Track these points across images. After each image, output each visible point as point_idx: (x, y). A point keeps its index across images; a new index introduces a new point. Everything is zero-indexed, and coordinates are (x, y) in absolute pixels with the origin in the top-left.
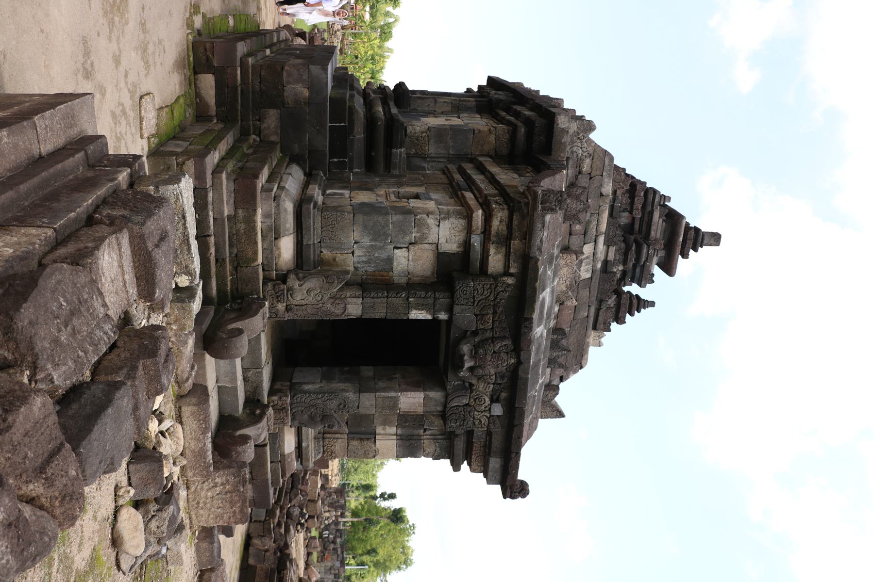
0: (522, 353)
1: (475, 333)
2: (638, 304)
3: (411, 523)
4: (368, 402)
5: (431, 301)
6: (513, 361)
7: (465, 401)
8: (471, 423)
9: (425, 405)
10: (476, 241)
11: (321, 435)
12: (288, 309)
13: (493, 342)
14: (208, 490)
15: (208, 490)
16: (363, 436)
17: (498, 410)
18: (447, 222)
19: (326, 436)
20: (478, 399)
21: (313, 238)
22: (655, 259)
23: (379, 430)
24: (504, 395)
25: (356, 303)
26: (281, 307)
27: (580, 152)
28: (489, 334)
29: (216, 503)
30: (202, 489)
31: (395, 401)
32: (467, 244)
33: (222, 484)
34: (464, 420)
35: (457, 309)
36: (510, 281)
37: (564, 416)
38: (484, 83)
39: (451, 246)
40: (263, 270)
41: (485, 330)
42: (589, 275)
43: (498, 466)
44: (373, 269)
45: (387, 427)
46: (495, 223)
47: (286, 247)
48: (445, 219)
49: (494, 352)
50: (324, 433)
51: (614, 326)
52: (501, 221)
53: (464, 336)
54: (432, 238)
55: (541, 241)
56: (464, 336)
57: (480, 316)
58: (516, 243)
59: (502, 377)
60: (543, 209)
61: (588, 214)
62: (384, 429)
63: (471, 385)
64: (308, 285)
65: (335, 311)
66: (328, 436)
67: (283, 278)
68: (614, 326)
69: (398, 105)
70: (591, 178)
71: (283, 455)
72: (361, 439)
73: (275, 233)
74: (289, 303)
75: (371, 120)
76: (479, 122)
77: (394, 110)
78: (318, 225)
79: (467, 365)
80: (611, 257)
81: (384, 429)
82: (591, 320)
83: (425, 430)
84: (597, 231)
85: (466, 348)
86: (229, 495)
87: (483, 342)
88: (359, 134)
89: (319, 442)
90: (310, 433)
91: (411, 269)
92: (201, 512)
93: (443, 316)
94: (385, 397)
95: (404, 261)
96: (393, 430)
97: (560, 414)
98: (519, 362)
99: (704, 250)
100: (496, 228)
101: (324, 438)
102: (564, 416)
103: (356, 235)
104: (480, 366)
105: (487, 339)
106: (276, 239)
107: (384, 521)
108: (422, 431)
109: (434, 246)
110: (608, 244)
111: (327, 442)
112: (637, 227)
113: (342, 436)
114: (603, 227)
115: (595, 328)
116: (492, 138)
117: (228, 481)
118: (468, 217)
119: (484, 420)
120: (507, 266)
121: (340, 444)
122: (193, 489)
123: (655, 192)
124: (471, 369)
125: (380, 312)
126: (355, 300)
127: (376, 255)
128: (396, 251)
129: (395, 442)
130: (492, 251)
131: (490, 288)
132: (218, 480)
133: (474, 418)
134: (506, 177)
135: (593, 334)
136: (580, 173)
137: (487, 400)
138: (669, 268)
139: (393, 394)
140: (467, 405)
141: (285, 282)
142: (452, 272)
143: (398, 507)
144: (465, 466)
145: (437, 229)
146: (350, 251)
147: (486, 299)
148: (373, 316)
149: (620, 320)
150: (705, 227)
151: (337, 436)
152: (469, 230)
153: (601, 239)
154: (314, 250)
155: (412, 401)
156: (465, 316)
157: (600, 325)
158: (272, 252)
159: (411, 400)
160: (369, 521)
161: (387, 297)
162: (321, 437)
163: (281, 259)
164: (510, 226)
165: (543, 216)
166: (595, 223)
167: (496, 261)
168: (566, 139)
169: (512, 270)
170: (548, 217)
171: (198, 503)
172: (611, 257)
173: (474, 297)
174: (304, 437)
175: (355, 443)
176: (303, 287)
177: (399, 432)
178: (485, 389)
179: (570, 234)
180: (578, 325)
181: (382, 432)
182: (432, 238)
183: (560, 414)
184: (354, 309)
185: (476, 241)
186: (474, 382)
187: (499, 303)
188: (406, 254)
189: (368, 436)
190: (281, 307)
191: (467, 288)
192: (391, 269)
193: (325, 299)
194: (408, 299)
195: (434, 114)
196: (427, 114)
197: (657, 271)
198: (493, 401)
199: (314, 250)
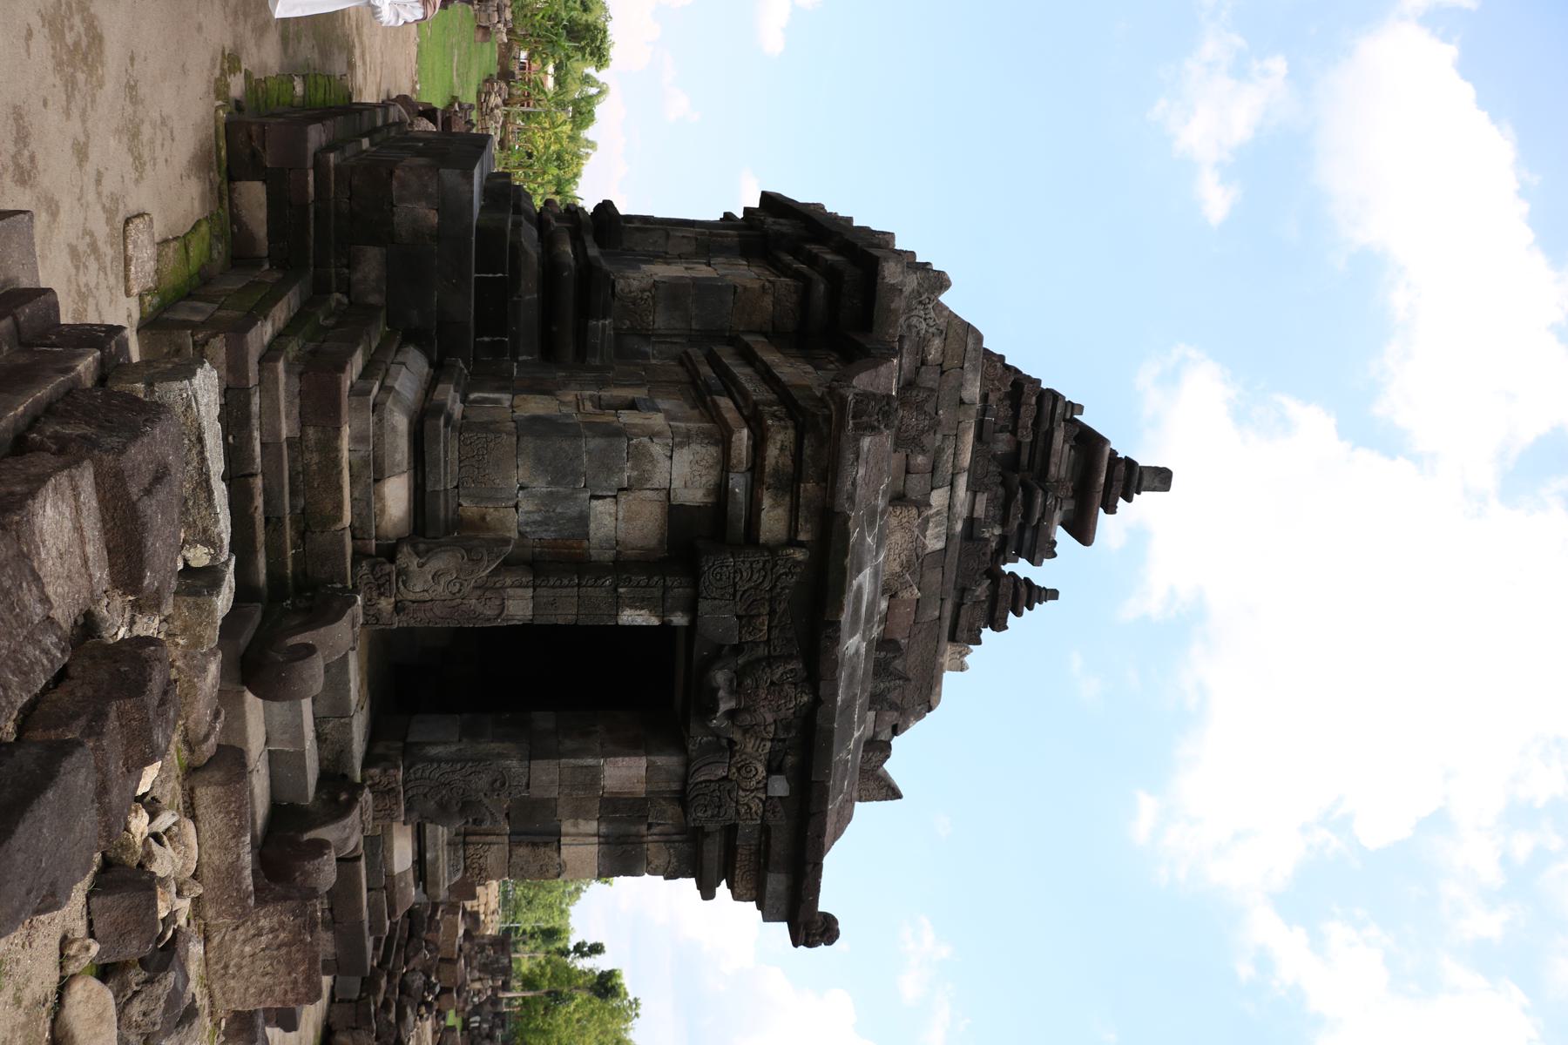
0: (822, 684)
1: (738, 649)
2: (1030, 595)
3: (631, 998)
4: (546, 776)
5: (657, 593)
6: (805, 699)
7: (721, 773)
8: (732, 812)
9: (648, 780)
10: (738, 484)
11: (460, 838)
12: (399, 608)
13: (770, 665)
14: (244, 942)
15: (244, 942)
16: (537, 839)
17: (780, 787)
18: (685, 450)
19: (469, 839)
20: (744, 767)
21: (444, 479)
22: (1058, 516)
23: (567, 827)
24: (790, 760)
25: (522, 598)
26: (386, 604)
27: (924, 326)
28: (762, 651)
29: (262, 965)
30: (234, 939)
31: (595, 773)
32: (721, 491)
33: (272, 930)
34: (720, 807)
35: (704, 606)
36: (800, 555)
37: (899, 796)
38: (755, 203)
39: (694, 494)
40: (353, 538)
41: (756, 644)
42: (940, 545)
43: (782, 888)
44: (553, 535)
45: (581, 822)
46: (772, 452)
47: (396, 496)
48: (681, 445)
49: (772, 683)
50: (466, 834)
51: (987, 633)
52: (782, 449)
53: (717, 654)
54: (660, 479)
55: (854, 484)
56: (717, 654)
57: (746, 619)
58: (808, 488)
59: (787, 728)
60: (857, 427)
61: (939, 437)
62: (576, 825)
63: (731, 742)
64: (437, 563)
65: (484, 611)
66: (473, 839)
67: (389, 552)
68: (987, 633)
69: (601, 244)
70: (942, 373)
71: (390, 876)
72: (534, 845)
73: (374, 471)
74: (400, 597)
75: (550, 267)
76: (744, 274)
77: (593, 251)
78: (454, 455)
79: (724, 707)
80: (980, 512)
81: (576, 825)
82: (947, 624)
83: (650, 826)
84: (954, 466)
85: (720, 677)
86: (284, 951)
88: (529, 292)
89: (456, 851)
91: (621, 536)
92: (232, 983)
93: (679, 619)
94: (575, 767)
95: (609, 521)
97: (893, 793)
98: (817, 701)
99: (1144, 499)
100: (773, 461)
101: (465, 844)
102: (899, 796)
103: (521, 473)
104: (747, 709)
105: (759, 660)
106: (376, 481)
107: (581, 997)
108: (644, 828)
109: (663, 494)
110: (974, 488)
111: (471, 850)
112: (1025, 458)
113: (499, 839)
114: (966, 459)
115: (953, 638)
116: (768, 301)
117: (282, 924)
119: (756, 806)
120: (793, 528)
121: (494, 854)
122: (216, 941)
123: (1055, 396)
124: (731, 714)
125: (566, 613)
126: (520, 591)
127: (559, 510)
128: (595, 503)
129: (595, 849)
130: (767, 502)
131: (763, 568)
132: (263, 923)
133: (737, 802)
134: (790, 370)
135: (949, 649)
136: (923, 363)
137: (761, 769)
138: (1083, 532)
139: (590, 761)
140: (725, 778)
141: (392, 560)
142: (695, 540)
143: (607, 968)
144: (723, 890)
145: (668, 463)
146: (511, 503)
147: (756, 588)
148: (553, 620)
149: (999, 625)
150: (1143, 460)
151: (489, 839)
152: (725, 464)
153: (962, 481)
154: (447, 501)
155: (624, 773)
156: (719, 619)
157: (962, 634)
158: (369, 504)
159: (624, 772)
160: (556, 997)
161: (579, 585)
162: (461, 841)
163: (387, 517)
164: (797, 456)
165: (857, 440)
166: (951, 451)
167: (773, 520)
168: (899, 304)
169: (802, 537)
170: (866, 442)
171: (226, 967)
172: (980, 512)
173: (735, 584)
174: (428, 843)
175: (522, 851)
176: (427, 568)
177: (603, 830)
178: (756, 751)
179: (907, 472)
180: (923, 634)
181: (572, 830)
182: (660, 479)
183: (895, 794)
184: (519, 607)
185: (738, 484)
186: (737, 736)
187: (779, 594)
188: (612, 509)
189: (546, 839)
190: (386, 604)
192: (587, 536)
193: (466, 590)
194: (615, 590)
195: (665, 258)
196: (653, 258)
197: (1061, 535)
198: (771, 771)
199: (447, 501)
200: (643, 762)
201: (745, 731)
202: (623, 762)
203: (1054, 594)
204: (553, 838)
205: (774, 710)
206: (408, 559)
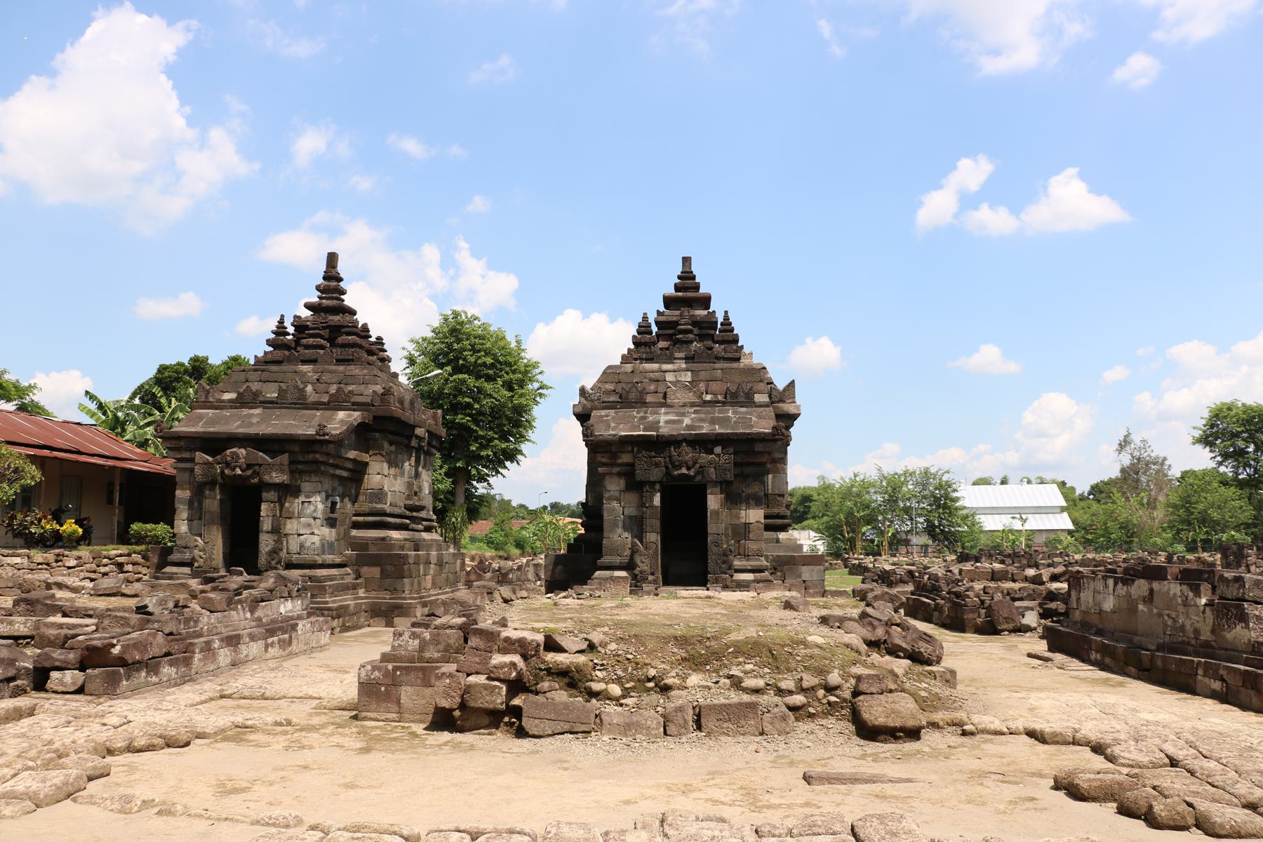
1: (667, 467)
10: (616, 470)
12: (653, 574)
17: (718, 450)
20: (710, 463)
21: (617, 560)
26: (651, 578)
32: (619, 475)
37: (793, 383)
39: (622, 483)
46: (604, 460)
54: (617, 494)
56: (668, 473)
57: (657, 465)
58: (613, 449)
64: (639, 563)
67: (635, 577)
79: (684, 471)
80: (682, 355)
87: (672, 463)
90: (737, 563)
93: (658, 486)
96: (743, 513)
98: (685, 440)
99: (695, 269)
102: (793, 383)
103: (616, 537)
110: (671, 359)
112: (670, 332)
114: (655, 366)
115: (738, 359)
118: (604, 475)
121: (752, 546)
124: (689, 469)
125: (657, 523)
130: (620, 461)
135: (745, 361)
150: (678, 269)
152: (610, 474)
155: (714, 501)
156: (656, 474)
162: (747, 557)
167: (625, 458)
172: (682, 355)
178: (705, 458)
182: (617, 494)
184: (654, 537)
191: (640, 474)
200: (709, 497)
201: (695, 463)
202: (709, 503)
203: (726, 312)
204: (747, 525)
205: (688, 454)
206: (637, 571)
